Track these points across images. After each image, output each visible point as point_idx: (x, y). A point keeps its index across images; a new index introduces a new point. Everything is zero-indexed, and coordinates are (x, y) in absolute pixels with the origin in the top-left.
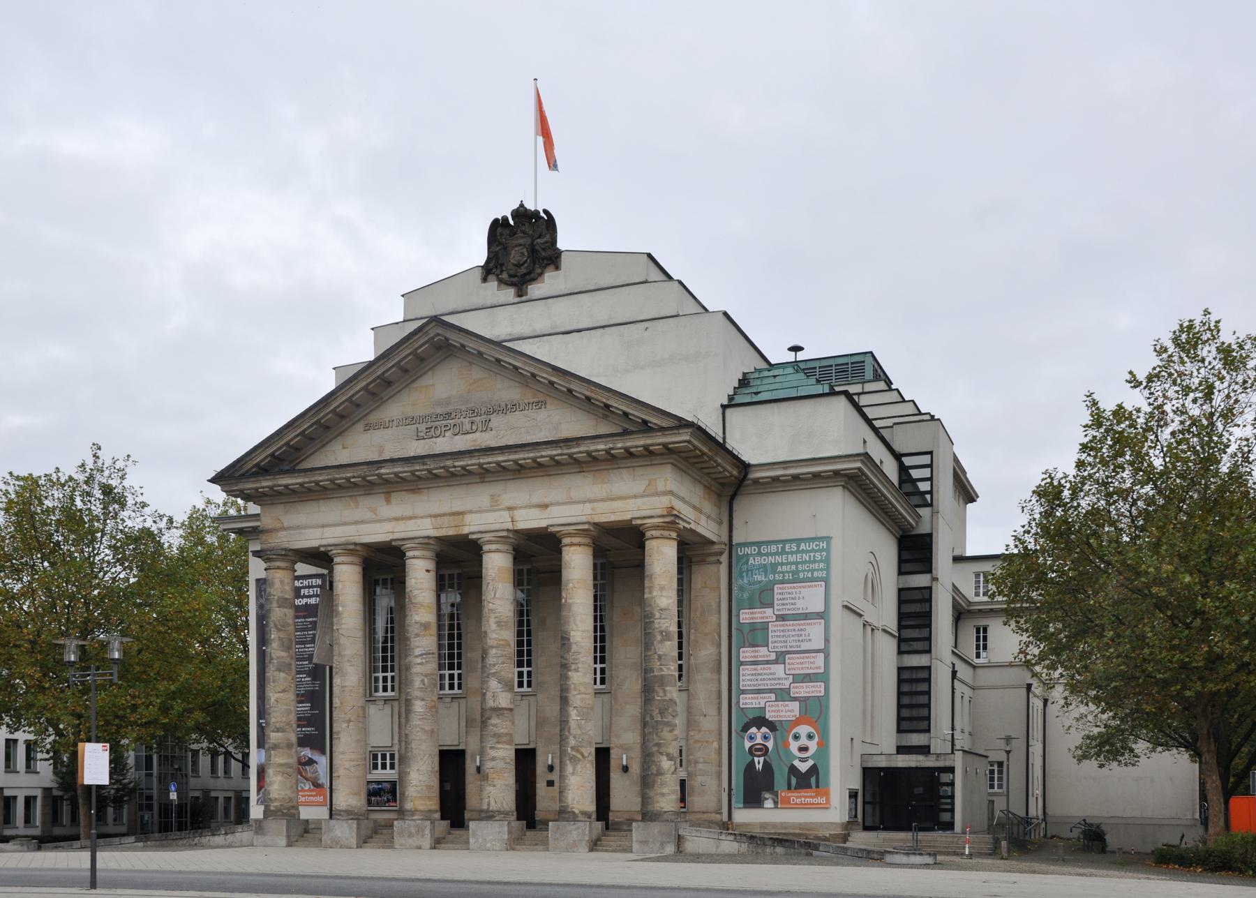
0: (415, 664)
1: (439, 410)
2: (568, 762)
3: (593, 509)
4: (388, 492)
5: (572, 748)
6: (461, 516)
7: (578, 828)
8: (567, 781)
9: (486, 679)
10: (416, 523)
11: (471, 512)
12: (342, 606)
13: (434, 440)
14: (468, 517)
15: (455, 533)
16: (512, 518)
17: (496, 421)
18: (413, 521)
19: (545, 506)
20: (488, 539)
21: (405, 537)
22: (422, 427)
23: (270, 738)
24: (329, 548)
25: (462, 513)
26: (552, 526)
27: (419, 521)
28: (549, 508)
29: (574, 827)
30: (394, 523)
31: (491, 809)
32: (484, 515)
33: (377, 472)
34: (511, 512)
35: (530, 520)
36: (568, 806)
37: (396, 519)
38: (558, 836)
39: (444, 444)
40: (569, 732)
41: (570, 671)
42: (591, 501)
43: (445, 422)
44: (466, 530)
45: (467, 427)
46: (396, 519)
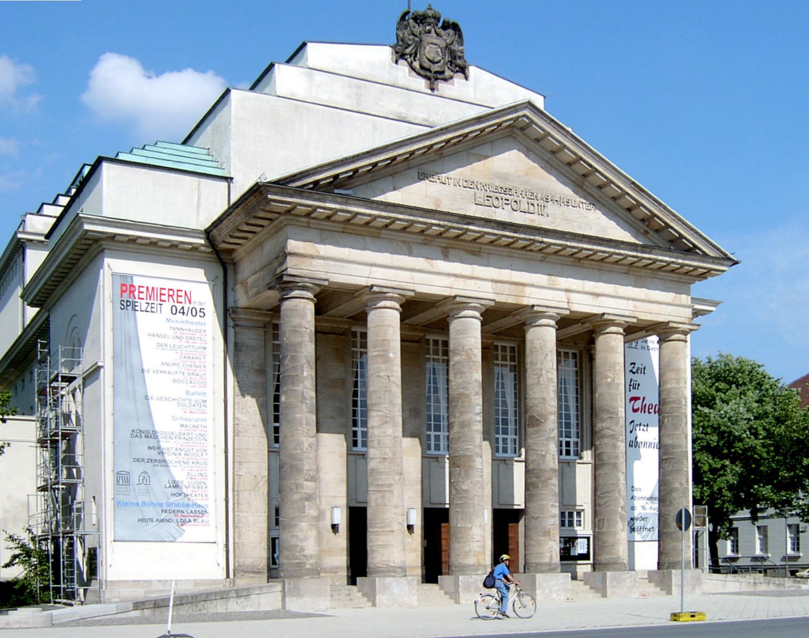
0: (476, 421)
1: (498, 183)
2: (619, 520)
3: (635, 307)
4: (446, 247)
5: (622, 508)
6: (521, 287)
7: (631, 577)
8: (618, 536)
9: (546, 442)
10: (476, 283)
11: (532, 286)
12: (393, 353)
13: (493, 208)
14: (528, 290)
15: (514, 302)
16: (568, 299)
17: (551, 208)
18: (474, 281)
19: (598, 295)
20: (551, 314)
21: (473, 296)
22: (481, 194)
23: (302, 488)
24: (385, 290)
25: (524, 285)
26: (608, 314)
27: (479, 282)
28: (600, 298)
29: (628, 575)
30: (452, 279)
31: (553, 562)
32: (543, 291)
33: (465, 227)
34: (568, 294)
35: (584, 305)
36: (619, 558)
37: (456, 276)
38: (615, 584)
39: (503, 215)
40: (619, 494)
41: (619, 441)
42: (634, 300)
43: (507, 197)
44: (526, 302)
45: (524, 206)
46: (456, 276)
